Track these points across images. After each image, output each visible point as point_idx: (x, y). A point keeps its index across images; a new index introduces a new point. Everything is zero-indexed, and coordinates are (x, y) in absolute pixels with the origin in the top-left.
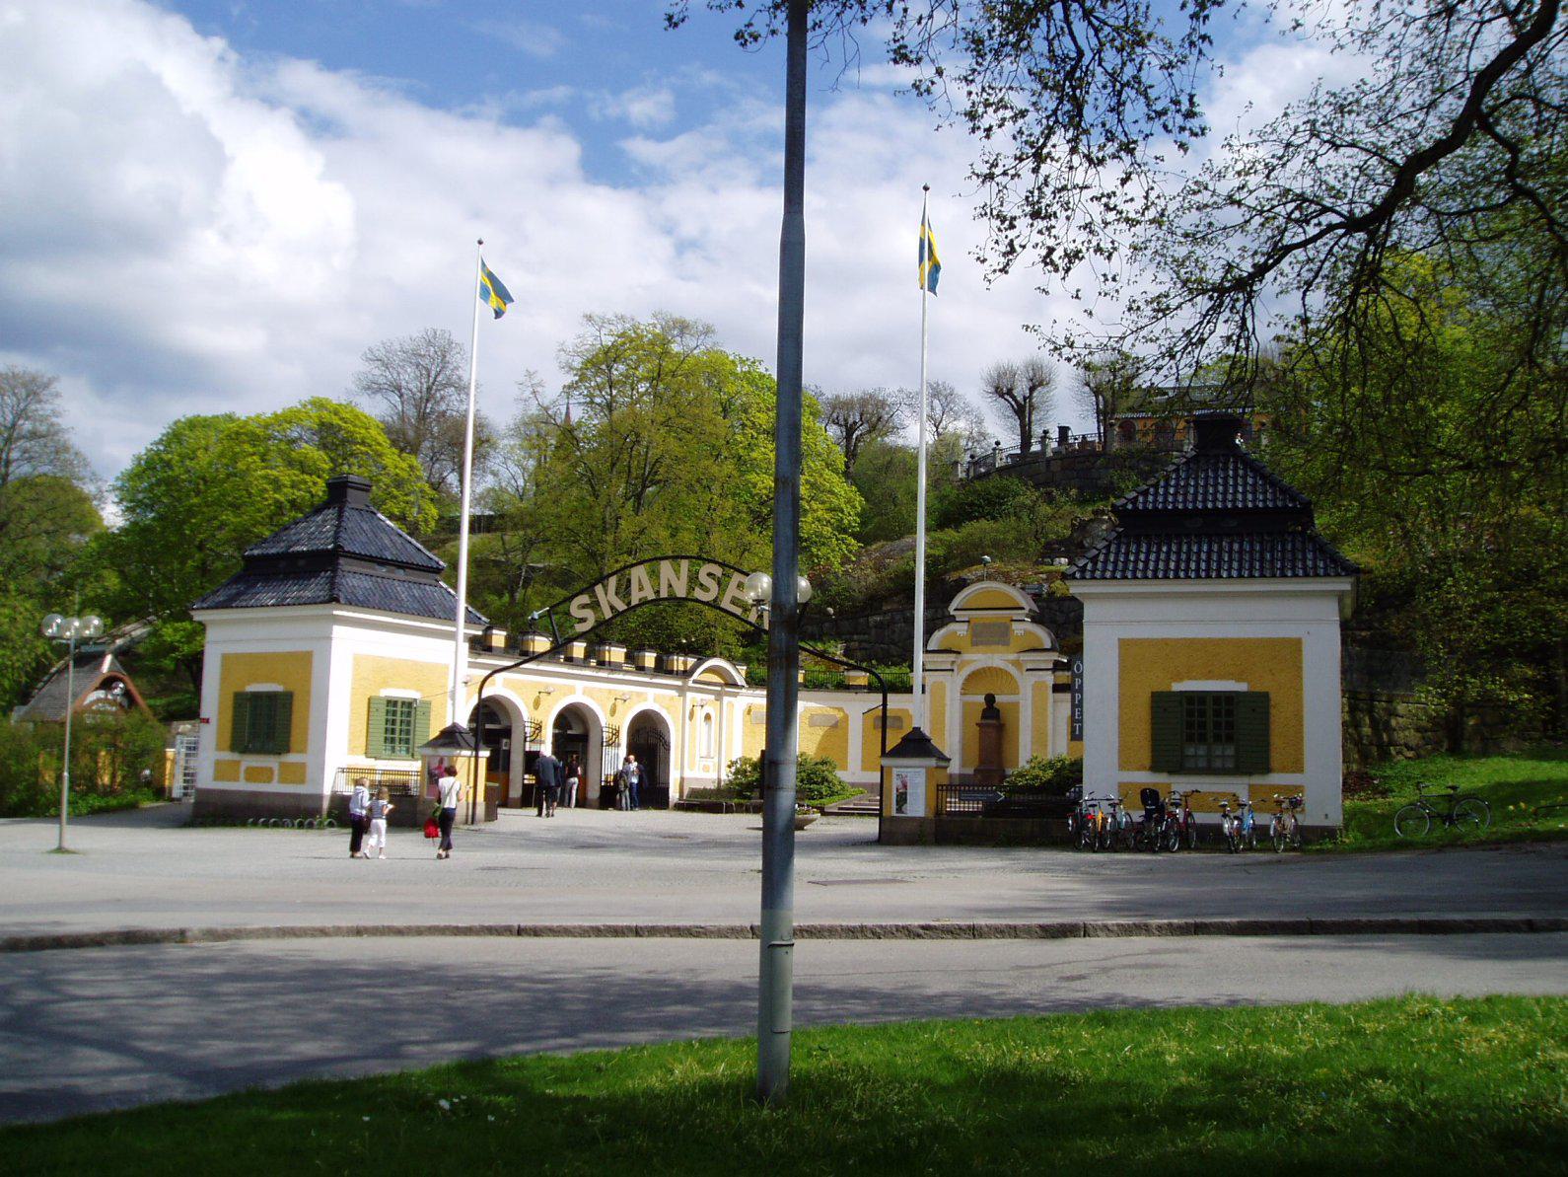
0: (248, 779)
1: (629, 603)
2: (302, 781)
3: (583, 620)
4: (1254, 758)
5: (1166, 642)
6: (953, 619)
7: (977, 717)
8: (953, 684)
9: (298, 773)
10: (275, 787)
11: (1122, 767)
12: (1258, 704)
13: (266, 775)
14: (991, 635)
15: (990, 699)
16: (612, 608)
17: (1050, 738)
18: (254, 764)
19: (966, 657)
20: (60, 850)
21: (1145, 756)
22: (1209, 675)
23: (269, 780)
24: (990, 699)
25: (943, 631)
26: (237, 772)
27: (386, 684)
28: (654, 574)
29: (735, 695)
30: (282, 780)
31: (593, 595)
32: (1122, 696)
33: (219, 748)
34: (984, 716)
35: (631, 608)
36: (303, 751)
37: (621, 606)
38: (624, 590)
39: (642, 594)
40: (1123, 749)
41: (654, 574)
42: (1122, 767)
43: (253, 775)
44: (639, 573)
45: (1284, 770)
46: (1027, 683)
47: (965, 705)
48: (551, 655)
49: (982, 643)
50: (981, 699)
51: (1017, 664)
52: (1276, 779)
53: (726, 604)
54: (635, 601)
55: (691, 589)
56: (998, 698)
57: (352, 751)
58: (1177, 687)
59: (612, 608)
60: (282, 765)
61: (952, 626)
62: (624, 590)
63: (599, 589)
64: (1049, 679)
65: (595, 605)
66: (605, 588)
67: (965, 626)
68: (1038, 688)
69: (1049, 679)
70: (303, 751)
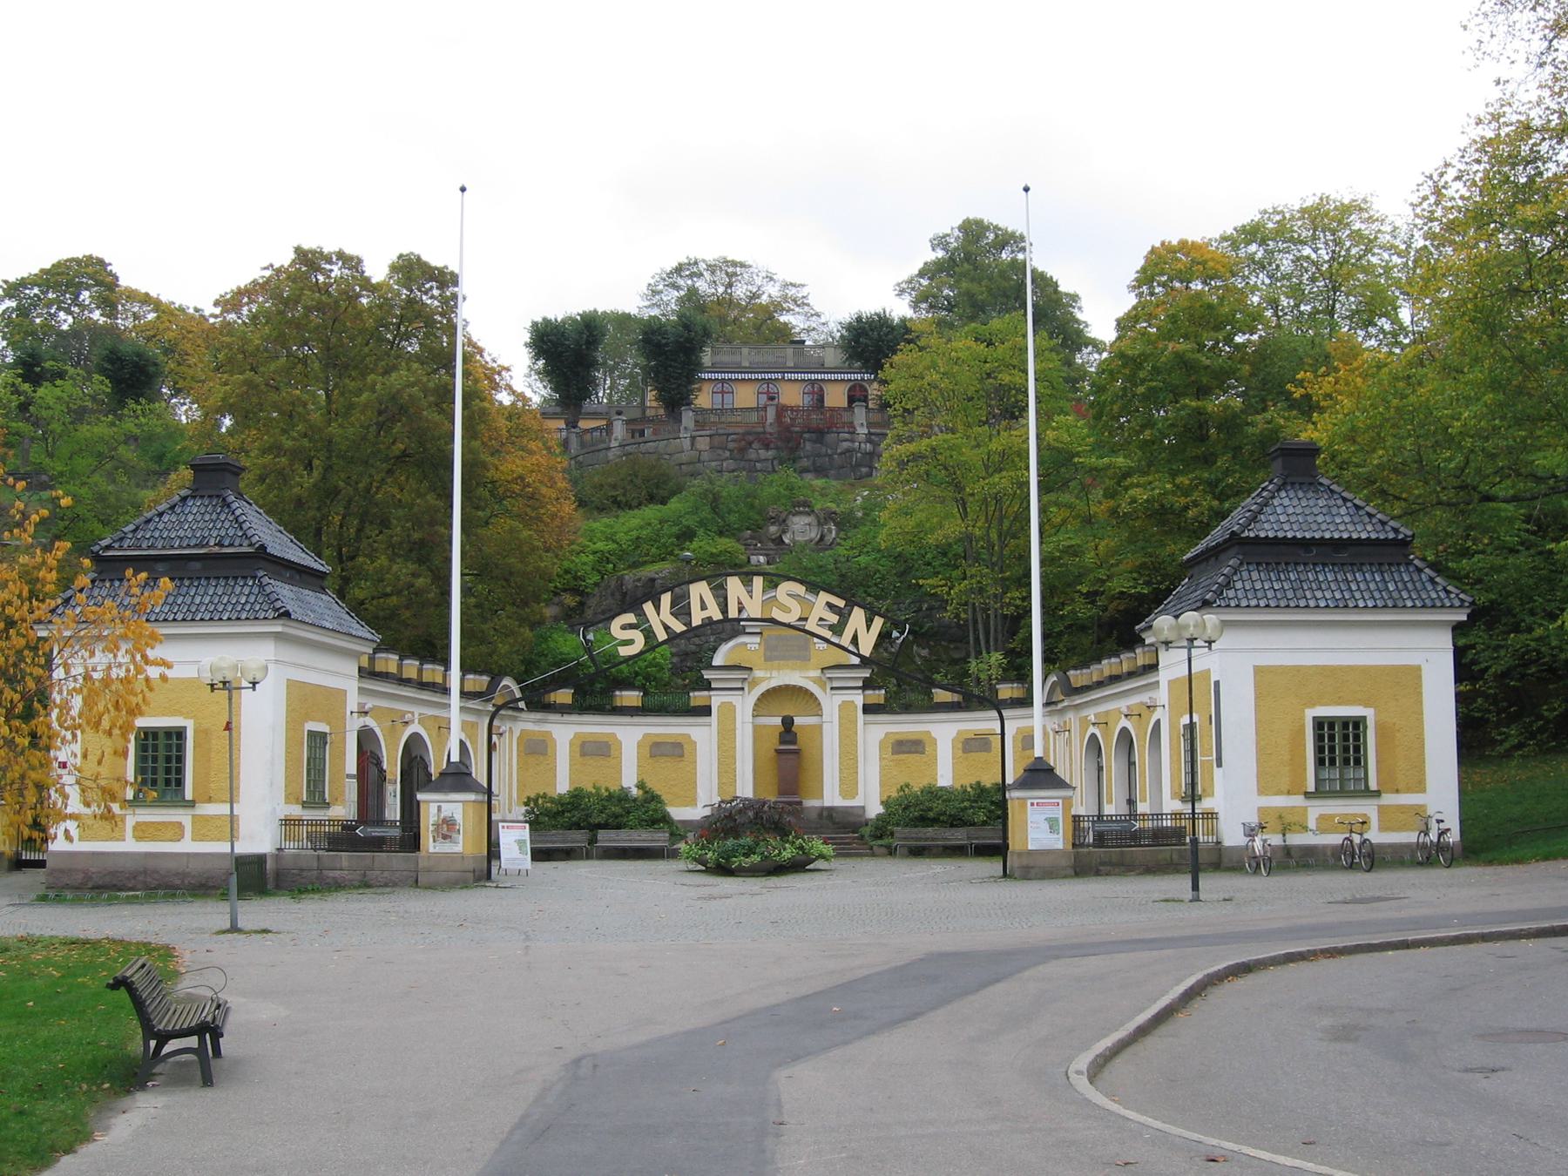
0: (138, 838)
1: (688, 624)
3: (630, 642)
7: (773, 742)
8: (745, 704)
10: (187, 846)
11: (1262, 791)
13: (177, 831)
15: (788, 722)
16: (666, 628)
17: (861, 766)
18: (141, 819)
19: (758, 673)
20: (234, 929)
23: (179, 837)
24: (788, 722)
25: (731, 643)
29: (515, 719)
30: (198, 837)
31: (641, 614)
32: (1258, 721)
34: (782, 742)
37: (678, 627)
38: (681, 610)
39: (705, 614)
42: (1262, 791)
43: (142, 832)
46: (831, 703)
47: (757, 729)
49: (777, 658)
50: (778, 721)
51: (818, 681)
53: (811, 626)
54: (696, 622)
56: (797, 721)
59: (666, 628)
62: (681, 610)
63: (648, 607)
64: (858, 699)
66: (657, 608)
67: (757, 639)
68: (844, 706)
69: (858, 699)
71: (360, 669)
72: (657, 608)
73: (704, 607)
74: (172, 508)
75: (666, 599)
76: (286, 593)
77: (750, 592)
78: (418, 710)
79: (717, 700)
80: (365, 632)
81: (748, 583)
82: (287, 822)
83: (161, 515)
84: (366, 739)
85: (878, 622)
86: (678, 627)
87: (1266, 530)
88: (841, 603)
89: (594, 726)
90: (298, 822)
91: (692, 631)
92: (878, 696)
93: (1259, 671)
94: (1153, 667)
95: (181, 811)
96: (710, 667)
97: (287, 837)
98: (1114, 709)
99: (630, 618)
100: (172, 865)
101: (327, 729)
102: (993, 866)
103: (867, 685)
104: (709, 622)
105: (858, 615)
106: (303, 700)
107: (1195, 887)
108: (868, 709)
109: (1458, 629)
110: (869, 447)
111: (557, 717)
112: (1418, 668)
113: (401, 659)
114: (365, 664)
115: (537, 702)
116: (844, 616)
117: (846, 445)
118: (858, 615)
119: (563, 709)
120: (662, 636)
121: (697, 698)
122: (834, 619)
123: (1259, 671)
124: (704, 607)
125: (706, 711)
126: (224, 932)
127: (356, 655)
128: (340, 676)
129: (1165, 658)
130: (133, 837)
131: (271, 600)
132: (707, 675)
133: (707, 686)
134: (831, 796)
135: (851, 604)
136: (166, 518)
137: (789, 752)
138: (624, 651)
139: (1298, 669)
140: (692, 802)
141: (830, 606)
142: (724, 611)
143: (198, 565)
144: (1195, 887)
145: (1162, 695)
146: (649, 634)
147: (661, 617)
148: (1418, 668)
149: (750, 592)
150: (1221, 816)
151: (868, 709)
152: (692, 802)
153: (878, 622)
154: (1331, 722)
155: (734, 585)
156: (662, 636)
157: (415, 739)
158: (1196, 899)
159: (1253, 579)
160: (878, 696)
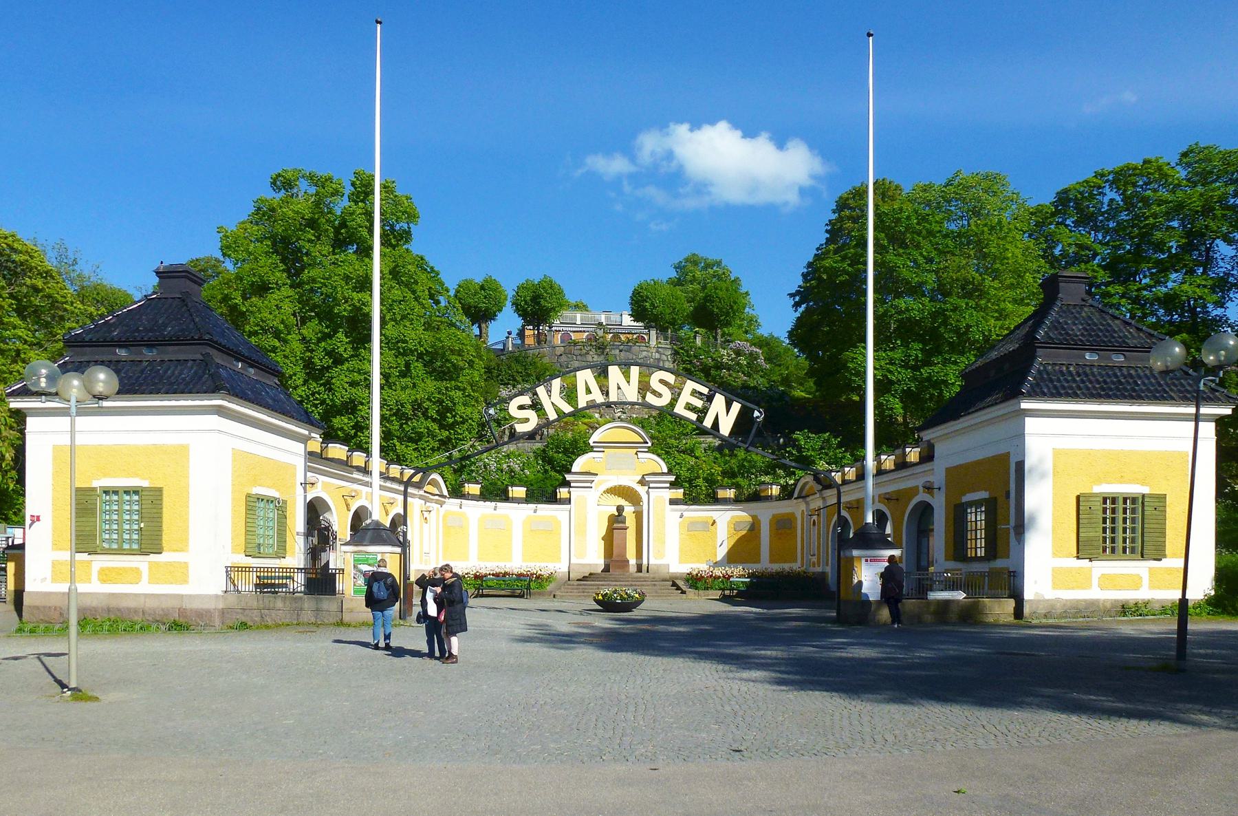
0: (103, 581)
2: (185, 581)
9: (180, 572)
10: (144, 587)
11: (1055, 555)
30: (153, 580)
33: (56, 546)
36: (182, 546)
37: (567, 409)
38: (570, 394)
39: (590, 397)
42: (1055, 555)
43: (105, 576)
48: (345, 464)
53: (680, 409)
54: (582, 403)
61: (591, 454)
62: (570, 394)
63: (541, 390)
65: (536, 406)
66: (549, 391)
72: (549, 391)
73: (589, 391)
81: (627, 376)
84: (314, 510)
86: (567, 409)
88: (705, 390)
91: (577, 413)
92: (679, 493)
96: (569, 472)
99: (525, 400)
100: (132, 604)
101: (277, 495)
103: (673, 485)
104: (592, 405)
105: (719, 400)
108: (673, 502)
110: (657, 356)
115: (457, 492)
116: (710, 399)
117: (645, 354)
118: (719, 400)
120: (552, 415)
121: (563, 493)
122: (699, 403)
124: (589, 391)
125: (568, 501)
129: (939, 450)
132: (568, 477)
133: (567, 484)
141: (695, 393)
147: (552, 398)
153: (736, 407)
156: (552, 415)
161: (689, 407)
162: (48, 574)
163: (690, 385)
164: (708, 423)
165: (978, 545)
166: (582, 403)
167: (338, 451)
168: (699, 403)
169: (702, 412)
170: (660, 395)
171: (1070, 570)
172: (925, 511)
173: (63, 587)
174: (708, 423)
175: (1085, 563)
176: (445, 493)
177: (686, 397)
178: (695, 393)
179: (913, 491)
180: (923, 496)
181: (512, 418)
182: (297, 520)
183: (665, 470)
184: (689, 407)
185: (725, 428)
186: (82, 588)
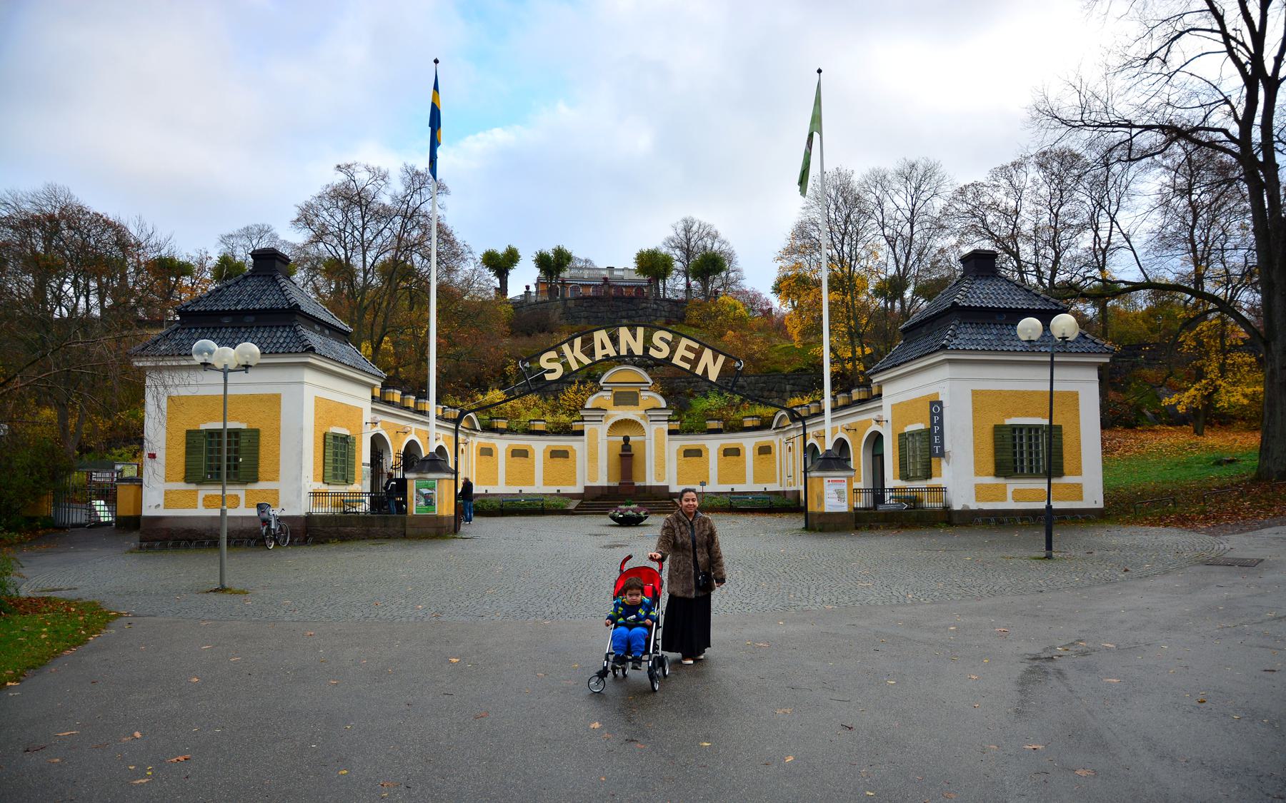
0: (207, 506)
3: (553, 371)
4: (1054, 468)
5: (1000, 393)
6: (601, 389)
7: (618, 450)
11: (977, 474)
12: (1053, 432)
14: (626, 398)
15: (626, 439)
16: (578, 362)
19: (609, 412)
20: (222, 589)
21: (991, 467)
22: (1027, 415)
24: (626, 439)
26: (195, 501)
27: (332, 424)
28: (615, 340)
34: (623, 450)
35: (595, 363)
37: (586, 361)
39: (605, 352)
40: (977, 462)
41: (615, 340)
42: (977, 474)
43: (208, 502)
44: (600, 336)
45: (1072, 474)
50: (621, 439)
51: (643, 417)
52: (1067, 479)
53: (676, 360)
54: (599, 355)
55: (646, 350)
57: (315, 479)
58: (1008, 422)
59: (578, 362)
60: (248, 493)
63: (566, 347)
64: (665, 426)
66: (572, 347)
69: (665, 426)
70: (275, 479)
71: (373, 397)
72: (572, 347)
73: (603, 347)
74: (237, 283)
75: (578, 341)
76: (315, 339)
77: (635, 338)
78: (414, 426)
79: (587, 427)
80: (377, 371)
82: (315, 494)
83: (228, 287)
84: (378, 444)
85: (721, 359)
86: (586, 361)
87: (975, 303)
88: (696, 346)
89: (521, 442)
90: (325, 494)
93: (975, 393)
94: (880, 395)
95: (238, 487)
97: (315, 504)
98: (865, 420)
99: (553, 354)
102: (798, 522)
105: (708, 354)
106: (325, 409)
107: (1049, 547)
108: (671, 432)
109: (1102, 369)
111: (497, 435)
112: (1076, 394)
113: (404, 394)
114: (377, 393)
116: (699, 355)
118: (708, 354)
119: (502, 432)
122: (691, 356)
123: (975, 393)
124: (603, 347)
125: (581, 433)
126: (216, 591)
127: (372, 387)
128: (358, 398)
130: (200, 505)
131: (301, 340)
134: (651, 480)
135: (704, 345)
136: (231, 289)
137: (627, 458)
138: (549, 377)
139: (1000, 392)
140: (574, 484)
142: (618, 352)
143: (252, 319)
144: (1049, 547)
145: (886, 413)
146: (566, 365)
148: (1076, 394)
149: (635, 338)
150: (950, 489)
151: (671, 432)
152: (574, 484)
153: (721, 359)
154: (1021, 428)
155: (624, 333)
156: (575, 367)
157: (412, 443)
158: (1049, 557)
159: (967, 335)
160: (676, 425)
161: (684, 359)
162: (161, 502)
163: (684, 342)
164: (699, 371)
165: (915, 466)
166: (599, 355)
167: (396, 395)
168: (691, 356)
169: (695, 363)
170: (660, 350)
171: (988, 487)
172: (876, 439)
173: (217, 513)
174: (699, 371)
175: (1001, 481)
176: (478, 427)
177: (681, 351)
178: (688, 348)
179: (868, 423)
180: (875, 427)
181: (541, 369)
182: (365, 455)
183: (664, 405)
184: (684, 359)
185: (713, 376)
186: (230, 512)
